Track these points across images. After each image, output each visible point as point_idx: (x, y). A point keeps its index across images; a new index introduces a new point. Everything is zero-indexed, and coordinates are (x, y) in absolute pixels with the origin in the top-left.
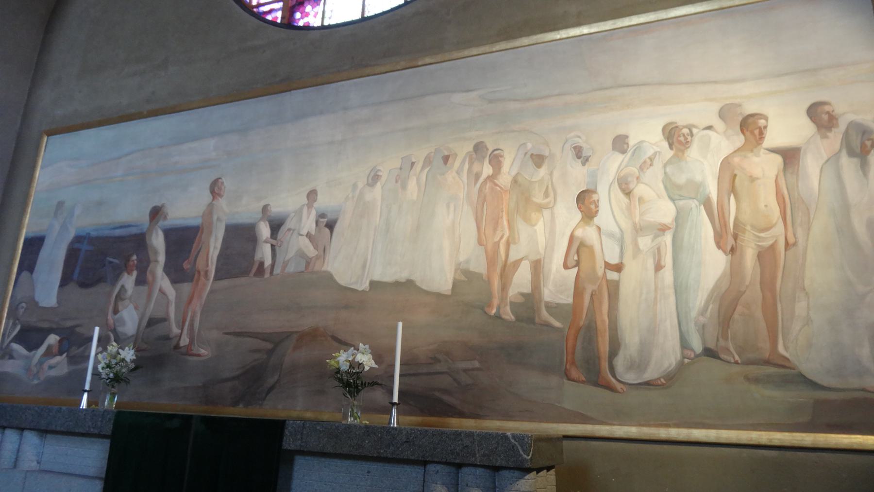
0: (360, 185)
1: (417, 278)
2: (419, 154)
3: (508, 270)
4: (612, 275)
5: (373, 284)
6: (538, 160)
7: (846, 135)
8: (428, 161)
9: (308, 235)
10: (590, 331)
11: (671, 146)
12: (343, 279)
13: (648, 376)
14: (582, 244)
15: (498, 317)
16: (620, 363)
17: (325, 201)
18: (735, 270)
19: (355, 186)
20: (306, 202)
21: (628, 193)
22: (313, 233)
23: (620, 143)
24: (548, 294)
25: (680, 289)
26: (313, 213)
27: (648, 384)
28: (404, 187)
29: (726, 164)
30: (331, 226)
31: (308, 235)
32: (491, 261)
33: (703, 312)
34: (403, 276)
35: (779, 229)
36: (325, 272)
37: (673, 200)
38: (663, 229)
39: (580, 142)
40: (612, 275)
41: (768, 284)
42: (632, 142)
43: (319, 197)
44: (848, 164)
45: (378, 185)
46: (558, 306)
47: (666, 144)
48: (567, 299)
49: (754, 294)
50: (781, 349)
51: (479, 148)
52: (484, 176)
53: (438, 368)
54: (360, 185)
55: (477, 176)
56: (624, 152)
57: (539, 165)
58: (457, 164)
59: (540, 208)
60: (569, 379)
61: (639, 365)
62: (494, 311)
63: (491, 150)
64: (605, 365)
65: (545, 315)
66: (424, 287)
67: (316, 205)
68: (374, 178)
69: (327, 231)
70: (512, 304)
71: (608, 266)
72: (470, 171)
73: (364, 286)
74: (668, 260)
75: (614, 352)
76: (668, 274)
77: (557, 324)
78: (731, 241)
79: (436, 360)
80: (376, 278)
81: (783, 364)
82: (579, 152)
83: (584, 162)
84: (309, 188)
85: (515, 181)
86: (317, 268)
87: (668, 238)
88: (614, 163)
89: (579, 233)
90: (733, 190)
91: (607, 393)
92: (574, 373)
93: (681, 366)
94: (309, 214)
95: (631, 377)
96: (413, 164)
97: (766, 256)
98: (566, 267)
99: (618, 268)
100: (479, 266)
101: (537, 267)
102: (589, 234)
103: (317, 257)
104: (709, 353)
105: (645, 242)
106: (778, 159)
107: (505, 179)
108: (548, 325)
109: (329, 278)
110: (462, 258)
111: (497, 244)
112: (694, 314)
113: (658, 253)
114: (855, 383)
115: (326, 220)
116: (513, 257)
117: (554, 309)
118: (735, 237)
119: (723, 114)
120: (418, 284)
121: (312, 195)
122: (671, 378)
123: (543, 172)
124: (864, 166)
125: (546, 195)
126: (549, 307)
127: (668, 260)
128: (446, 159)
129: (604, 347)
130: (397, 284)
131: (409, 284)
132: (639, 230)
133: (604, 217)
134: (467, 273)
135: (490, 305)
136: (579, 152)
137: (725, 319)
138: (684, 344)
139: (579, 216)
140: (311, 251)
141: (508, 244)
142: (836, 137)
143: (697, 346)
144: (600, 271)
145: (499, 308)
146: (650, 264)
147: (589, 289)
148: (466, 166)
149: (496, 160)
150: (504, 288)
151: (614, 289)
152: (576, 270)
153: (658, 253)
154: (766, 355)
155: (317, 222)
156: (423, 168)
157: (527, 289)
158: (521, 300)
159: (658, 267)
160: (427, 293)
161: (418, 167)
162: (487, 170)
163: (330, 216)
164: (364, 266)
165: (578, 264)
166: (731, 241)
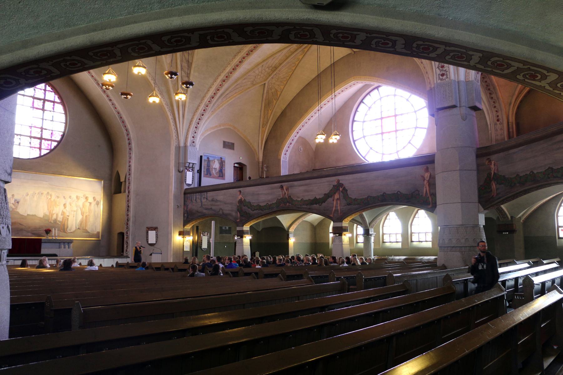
0: (24, 195)
1: (37, 214)
2: (37, 192)
3: (52, 215)
4: (68, 217)
5: (28, 215)
6: (58, 197)
7: (96, 202)
8: (38, 193)
9: (13, 204)
10: (64, 225)
11: (77, 199)
12: (21, 214)
13: (71, 231)
14: (64, 212)
15: (51, 222)
16: (68, 229)
17: (16, 197)
18: (83, 218)
19: (23, 195)
20: (11, 196)
21: (71, 205)
22: (14, 203)
23: (70, 197)
24: (59, 219)
25: (76, 220)
26: (14, 200)
27: (71, 232)
28: (34, 197)
29: (83, 203)
30: (18, 202)
31: (13, 204)
32: (50, 213)
33: (79, 223)
34: (34, 214)
35: (88, 213)
36: (17, 211)
37: (76, 207)
38: (75, 211)
39: (64, 195)
40: (68, 217)
41: (86, 221)
42: (72, 197)
43: (15, 196)
44: (96, 205)
45: (28, 196)
46: (60, 221)
47: (76, 199)
48: (61, 220)
49: (84, 221)
50: (86, 228)
51: (48, 193)
52: (49, 198)
53: (41, 230)
54: (24, 195)
55: (48, 198)
56: (70, 198)
57: (58, 198)
58: (44, 195)
59: (58, 205)
60: (61, 231)
61: (70, 230)
62: (50, 221)
63: (50, 194)
64: (66, 230)
65: (58, 222)
66: (38, 216)
67: (14, 198)
68: (27, 195)
69: (17, 203)
70: (53, 220)
71: (67, 216)
72: (46, 197)
73: (26, 215)
74: (75, 216)
75: (67, 228)
76: (75, 217)
77: (59, 224)
78: (83, 214)
79: (40, 228)
80: (29, 213)
81: (86, 230)
82: (64, 197)
83: (65, 199)
84: (13, 194)
85: (54, 200)
86: (15, 210)
87: (75, 213)
88: (69, 200)
89: (64, 210)
90: (84, 207)
91: (66, 234)
92: (62, 231)
93: (75, 230)
94: (13, 199)
95: (69, 232)
96: (36, 193)
97: (86, 216)
98: (61, 215)
99: (68, 216)
100: (48, 214)
101: (57, 215)
102: (65, 211)
103: (15, 208)
104: (79, 229)
105: (72, 213)
106: (89, 204)
107: (52, 199)
108: (58, 224)
109: (18, 213)
110: (45, 212)
111: (51, 210)
112: (77, 223)
113: (74, 215)
114: (93, 232)
115: (16, 201)
116: (53, 213)
117: (59, 221)
118: (83, 213)
119: (84, 196)
120: (37, 215)
121: (13, 195)
122: (74, 231)
123: (58, 199)
124: (98, 206)
125: (59, 203)
126: (59, 221)
127: (75, 216)
128: (42, 194)
129: (66, 227)
130: (33, 215)
131: (35, 215)
132: (72, 211)
133: (67, 208)
134: (45, 214)
135: (49, 220)
136: (64, 197)
137: (81, 224)
138: (76, 227)
139: (64, 207)
140: (13, 207)
141: (53, 210)
142: (95, 202)
143: (77, 228)
144: (66, 216)
145: (51, 220)
146: (73, 216)
147: (65, 219)
148: (46, 195)
149: (51, 196)
150: (52, 217)
151: (68, 219)
152: (62, 216)
153: (74, 215)
154: (85, 229)
155: (15, 201)
156: (38, 194)
157: (55, 218)
158: (54, 220)
159: (74, 217)
160: (38, 217)
161: (36, 194)
162: (49, 197)
163: (18, 201)
164: (26, 211)
165: (63, 215)
166: (83, 214)
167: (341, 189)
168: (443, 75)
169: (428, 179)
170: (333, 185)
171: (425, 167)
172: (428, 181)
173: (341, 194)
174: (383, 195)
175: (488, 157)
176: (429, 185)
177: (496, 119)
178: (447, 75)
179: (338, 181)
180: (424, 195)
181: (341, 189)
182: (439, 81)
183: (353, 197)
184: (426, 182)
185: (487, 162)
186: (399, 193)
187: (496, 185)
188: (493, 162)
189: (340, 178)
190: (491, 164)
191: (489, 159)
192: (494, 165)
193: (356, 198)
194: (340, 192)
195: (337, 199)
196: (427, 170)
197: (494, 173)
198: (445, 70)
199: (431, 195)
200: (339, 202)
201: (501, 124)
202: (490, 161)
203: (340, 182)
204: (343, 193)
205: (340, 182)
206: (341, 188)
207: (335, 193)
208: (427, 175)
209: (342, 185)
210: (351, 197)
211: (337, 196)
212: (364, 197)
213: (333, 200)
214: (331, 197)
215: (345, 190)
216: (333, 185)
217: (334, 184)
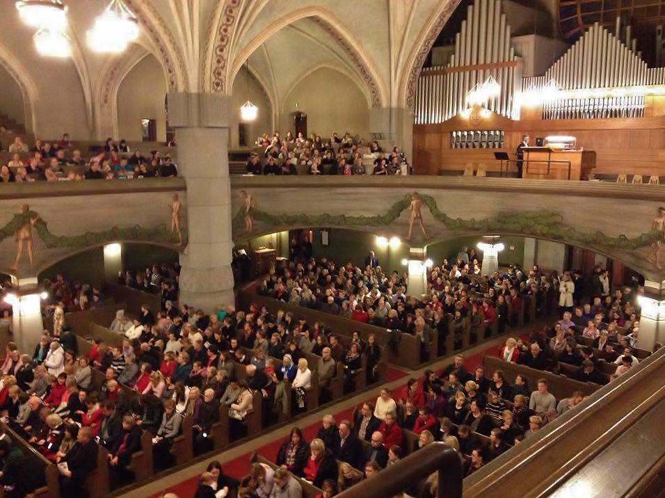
167: (32, 222)
168: (218, 84)
169: (177, 210)
170: (15, 215)
171: (174, 195)
172: (178, 213)
173: (34, 229)
174: (112, 231)
175: (244, 189)
176: (179, 218)
177: (102, 100)
178: (222, 86)
179: (27, 207)
180: (172, 229)
181: (32, 222)
182: (213, 91)
183: (58, 234)
184: (174, 214)
185: (241, 195)
186: (137, 227)
187: (252, 221)
188: (249, 197)
189: (32, 202)
190: (247, 197)
191: (243, 191)
192: (252, 199)
193: (63, 236)
194: (32, 227)
195: (26, 239)
196: (176, 198)
197: (251, 208)
198: (221, 80)
199: (181, 230)
200: (29, 243)
201: (109, 107)
202: (245, 194)
203: (31, 209)
204: (37, 228)
205: (31, 209)
206: (34, 219)
207: (20, 229)
208: (176, 205)
209: (34, 215)
210: (54, 234)
211: (24, 233)
212: (81, 234)
213: (17, 241)
214: (12, 234)
215: (41, 223)
216: (15, 215)
217: (16, 213)
